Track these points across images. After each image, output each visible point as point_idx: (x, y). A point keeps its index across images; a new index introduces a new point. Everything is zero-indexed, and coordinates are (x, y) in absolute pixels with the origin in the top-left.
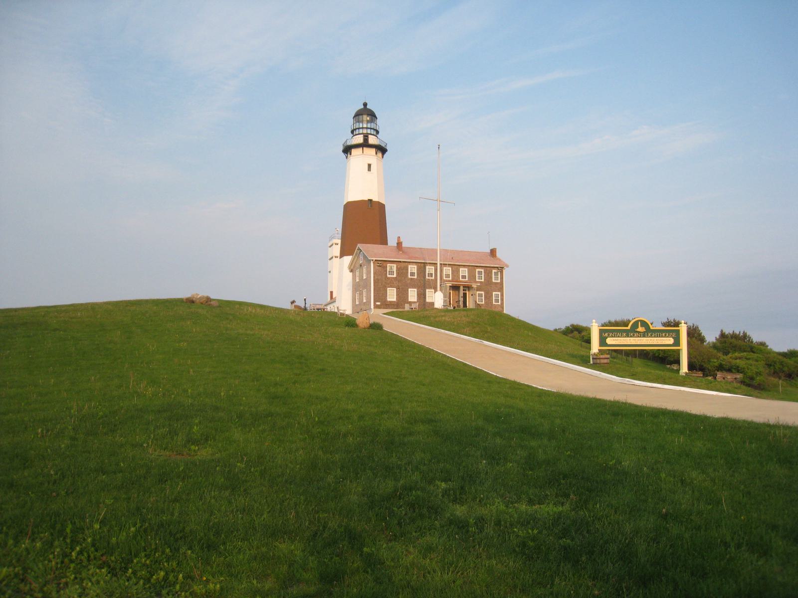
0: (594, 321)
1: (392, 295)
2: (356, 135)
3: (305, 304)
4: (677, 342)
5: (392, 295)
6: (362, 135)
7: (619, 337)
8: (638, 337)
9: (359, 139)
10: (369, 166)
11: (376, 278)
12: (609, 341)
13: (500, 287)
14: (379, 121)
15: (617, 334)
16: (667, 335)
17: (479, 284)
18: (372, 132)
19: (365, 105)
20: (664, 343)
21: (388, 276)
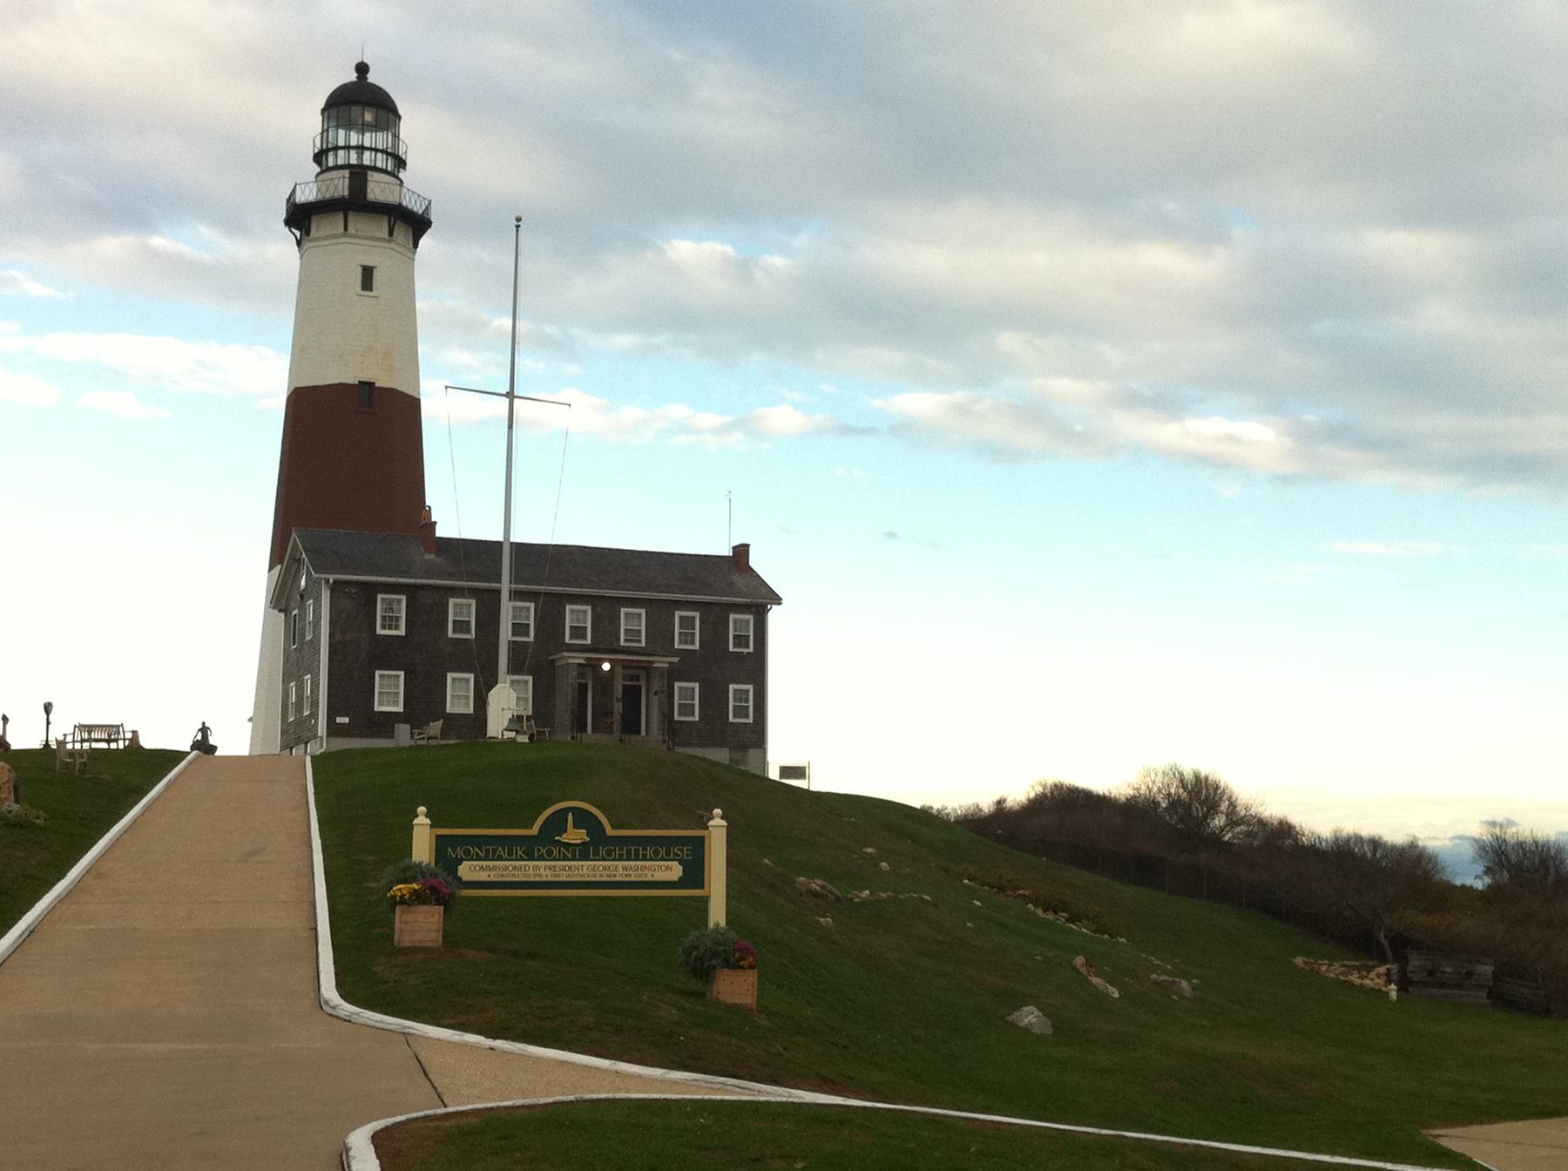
0: (422, 809)
1: (389, 692)
2: (329, 169)
3: (48, 723)
4: (695, 874)
5: (389, 692)
6: (346, 173)
7: (500, 858)
8: (565, 859)
9: (340, 185)
10: (368, 274)
11: (338, 637)
12: (468, 870)
13: (754, 668)
14: (405, 128)
15: (494, 851)
16: (662, 852)
17: (676, 660)
18: (380, 161)
19: (362, 69)
20: (649, 878)
21: (380, 631)
